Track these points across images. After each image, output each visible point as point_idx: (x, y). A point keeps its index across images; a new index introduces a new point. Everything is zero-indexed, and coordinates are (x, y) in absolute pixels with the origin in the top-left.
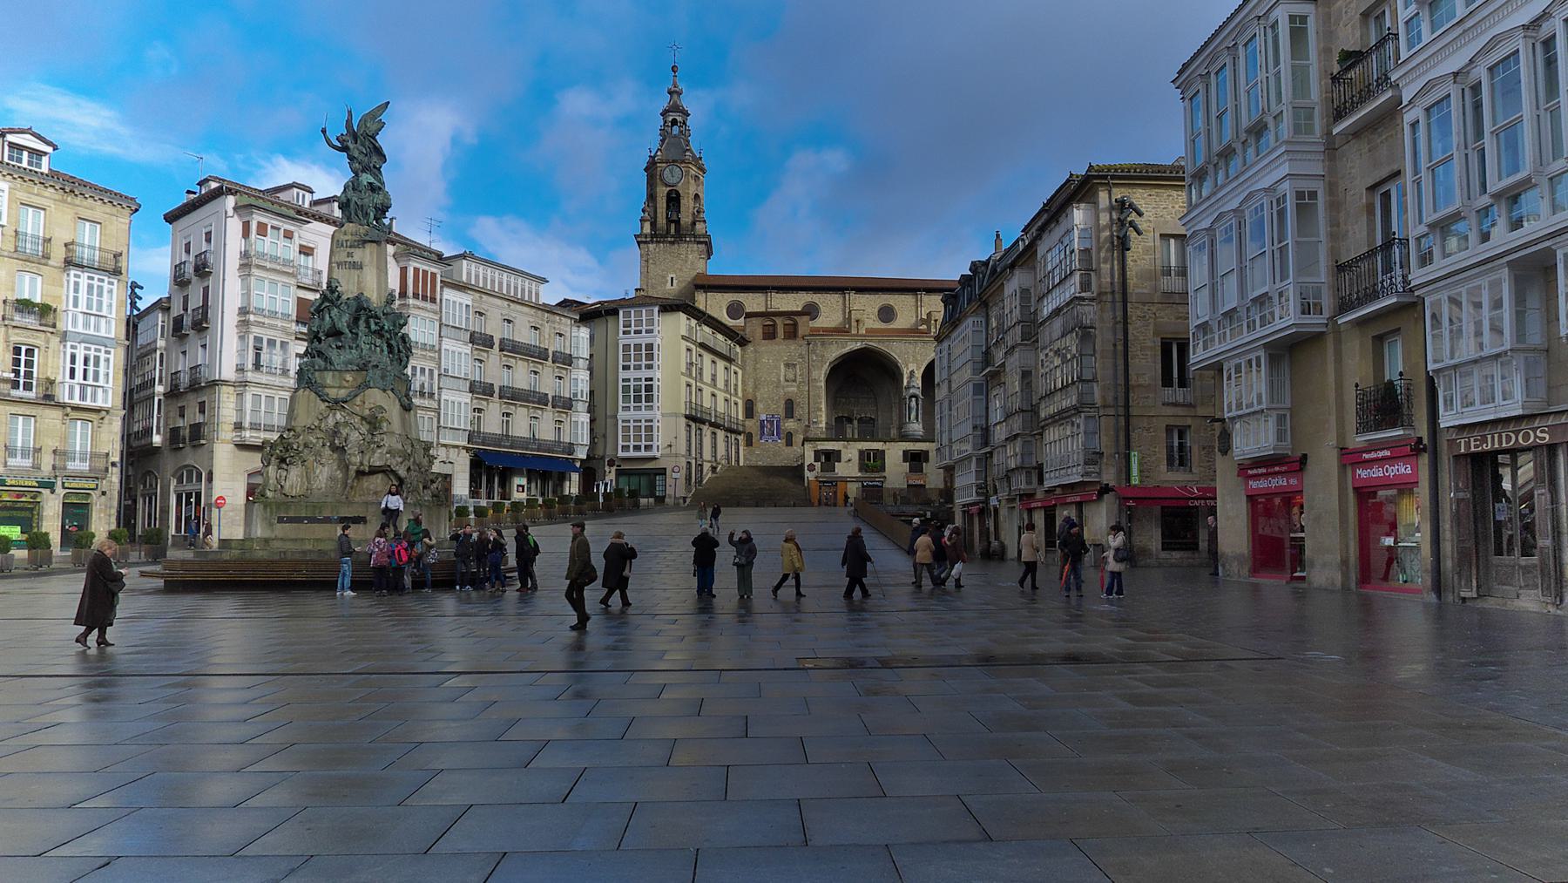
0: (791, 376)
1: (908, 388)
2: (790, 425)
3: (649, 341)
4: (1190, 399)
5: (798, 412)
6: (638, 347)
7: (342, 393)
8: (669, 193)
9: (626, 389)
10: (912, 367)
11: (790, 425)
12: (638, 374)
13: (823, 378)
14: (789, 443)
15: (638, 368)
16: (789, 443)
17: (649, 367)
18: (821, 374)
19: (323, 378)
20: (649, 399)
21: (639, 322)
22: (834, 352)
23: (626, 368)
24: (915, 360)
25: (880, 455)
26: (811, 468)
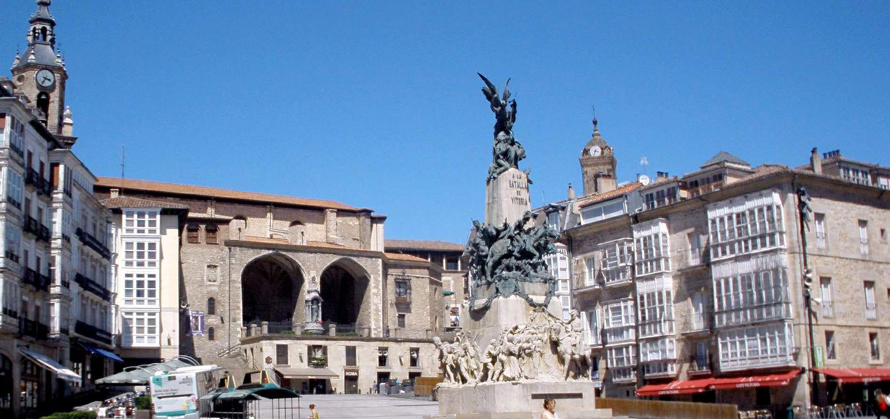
0: (213, 277)
1: (309, 292)
2: (213, 321)
3: (152, 241)
4: (831, 314)
5: (219, 309)
6: (141, 246)
7: (540, 299)
8: (39, 96)
9: (129, 284)
10: (313, 273)
11: (213, 321)
12: (140, 270)
13: (240, 280)
14: (211, 337)
15: (140, 264)
16: (211, 337)
17: (152, 264)
18: (237, 277)
19: (523, 287)
20: (152, 294)
21: (141, 224)
22: (252, 256)
23: (129, 264)
24: (315, 268)
25: (325, 349)
26: (268, 360)
